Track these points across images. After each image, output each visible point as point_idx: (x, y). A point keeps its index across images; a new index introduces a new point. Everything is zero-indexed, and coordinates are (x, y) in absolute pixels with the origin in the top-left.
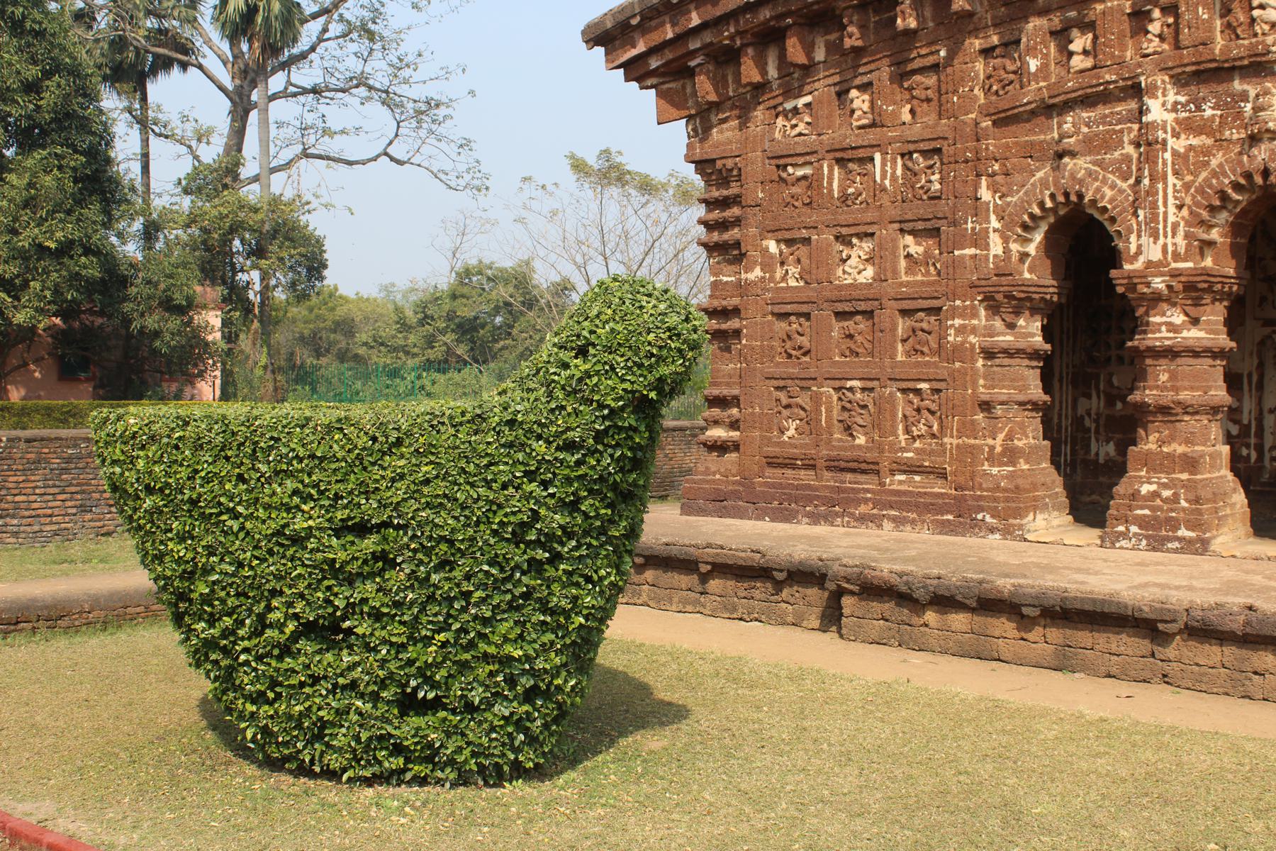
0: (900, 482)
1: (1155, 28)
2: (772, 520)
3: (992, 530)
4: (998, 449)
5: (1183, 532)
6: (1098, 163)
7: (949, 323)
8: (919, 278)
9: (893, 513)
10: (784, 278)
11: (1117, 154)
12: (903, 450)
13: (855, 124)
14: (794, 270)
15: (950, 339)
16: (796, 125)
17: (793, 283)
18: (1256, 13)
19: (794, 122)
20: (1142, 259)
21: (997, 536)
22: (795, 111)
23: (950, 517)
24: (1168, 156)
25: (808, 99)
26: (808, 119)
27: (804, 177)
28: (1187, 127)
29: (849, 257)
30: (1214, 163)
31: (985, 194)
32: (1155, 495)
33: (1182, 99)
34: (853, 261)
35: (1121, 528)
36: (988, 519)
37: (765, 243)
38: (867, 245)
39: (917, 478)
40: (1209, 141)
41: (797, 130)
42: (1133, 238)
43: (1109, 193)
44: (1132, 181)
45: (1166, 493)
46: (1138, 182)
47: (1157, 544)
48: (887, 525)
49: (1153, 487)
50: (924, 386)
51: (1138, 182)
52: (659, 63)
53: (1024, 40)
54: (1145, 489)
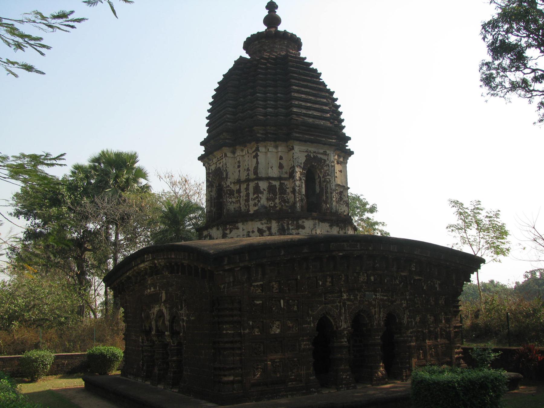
0: (291, 385)
1: (343, 279)
2: (255, 402)
3: (315, 392)
4: (312, 373)
5: (352, 385)
6: (332, 306)
7: (302, 343)
8: (291, 332)
9: (290, 393)
10: (254, 333)
11: (336, 304)
12: (291, 376)
13: (274, 291)
14: (257, 330)
15: (303, 347)
16: (257, 290)
17: (257, 334)
18: (360, 279)
19: (257, 289)
20: (342, 327)
21: (316, 393)
22: (257, 286)
23: (304, 391)
24: (347, 306)
25: (262, 283)
26: (261, 289)
27: (260, 304)
28: (348, 300)
29: (273, 326)
30: (353, 307)
31: (310, 312)
32: (346, 378)
33: (347, 294)
34: (274, 328)
35: (341, 386)
36: (314, 390)
37: (249, 322)
38: (277, 323)
39: (294, 383)
40: (352, 303)
41: (257, 292)
42: (340, 323)
43: (335, 314)
44: (339, 310)
45: (348, 377)
46: (340, 310)
47: (348, 389)
48: (289, 396)
49: (345, 376)
50: (296, 359)
51: (340, 310)
52: (229, 268)
53: (318, 277)
54: (344, 377)
